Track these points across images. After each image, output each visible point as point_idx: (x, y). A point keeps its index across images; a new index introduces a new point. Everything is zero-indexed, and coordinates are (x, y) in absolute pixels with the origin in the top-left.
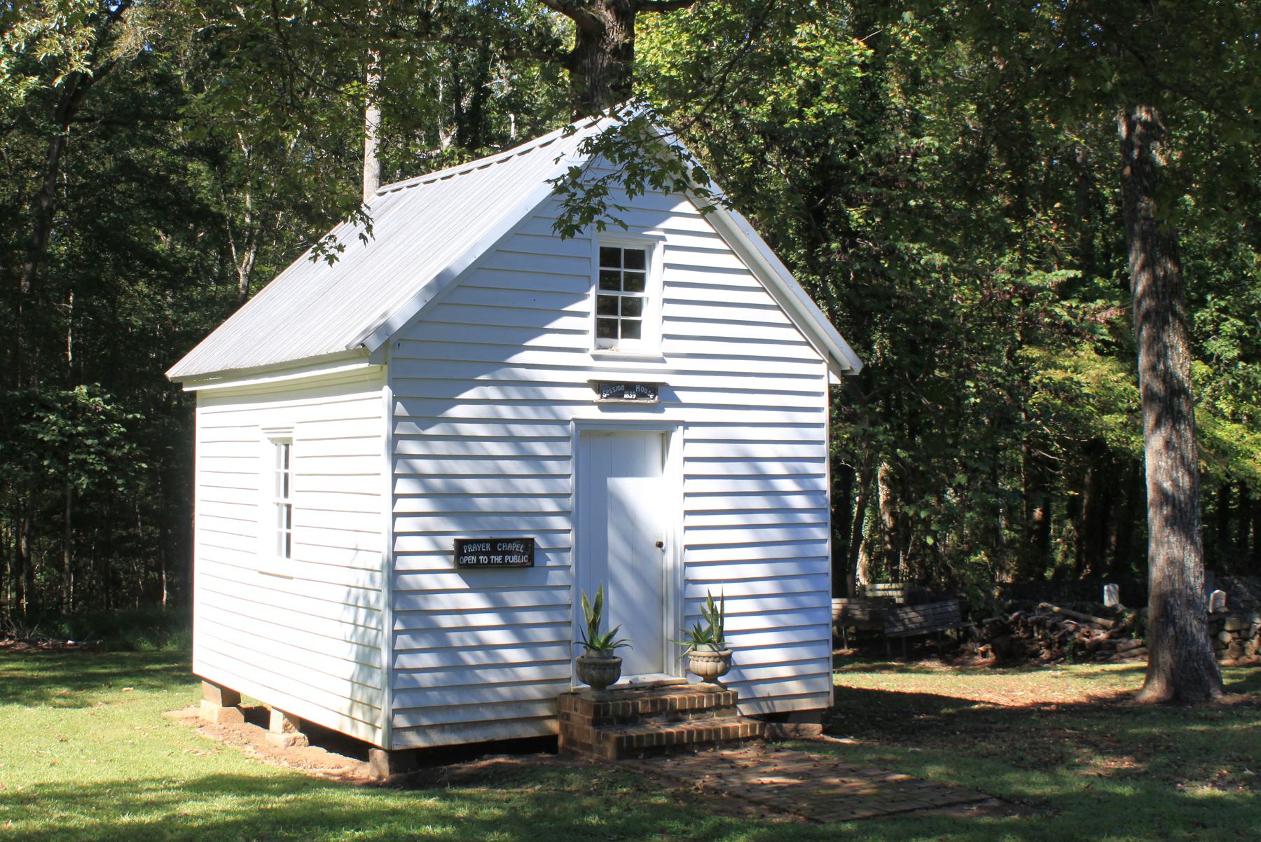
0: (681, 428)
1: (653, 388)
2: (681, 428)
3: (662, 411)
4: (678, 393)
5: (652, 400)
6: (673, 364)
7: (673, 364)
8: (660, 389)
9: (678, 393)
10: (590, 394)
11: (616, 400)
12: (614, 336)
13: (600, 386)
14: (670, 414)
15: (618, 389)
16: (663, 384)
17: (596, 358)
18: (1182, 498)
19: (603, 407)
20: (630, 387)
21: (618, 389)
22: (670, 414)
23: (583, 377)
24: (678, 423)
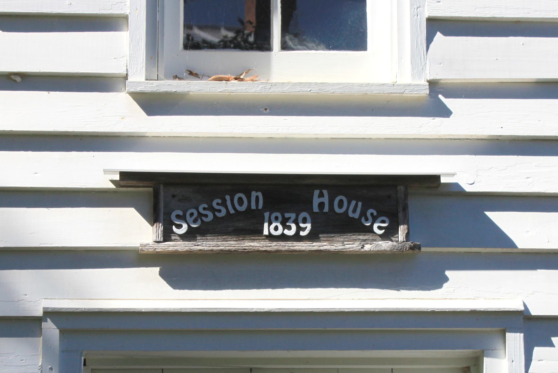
0: (515, 340)
1: (386, 198)
2: (515, 340)
3: (436, 281)
4: (501, 219)
5: (277, 233)
6: (471, 118)
7: (471, 118)
8: (415, 204)
9: (501, 219)
10: (132, 228)
11: (231, 244)
12: (262, 43)
13: (160, 195)
14: (467, 290)
15: (238, 203)
16: (431, 181)
17: (152, 104)
18: (160, 225)
19: (178, 271)
20: (286, 194)
21: (238, 203)
22: (467, 290)
23: (96, 170)
24: (504, 321)
